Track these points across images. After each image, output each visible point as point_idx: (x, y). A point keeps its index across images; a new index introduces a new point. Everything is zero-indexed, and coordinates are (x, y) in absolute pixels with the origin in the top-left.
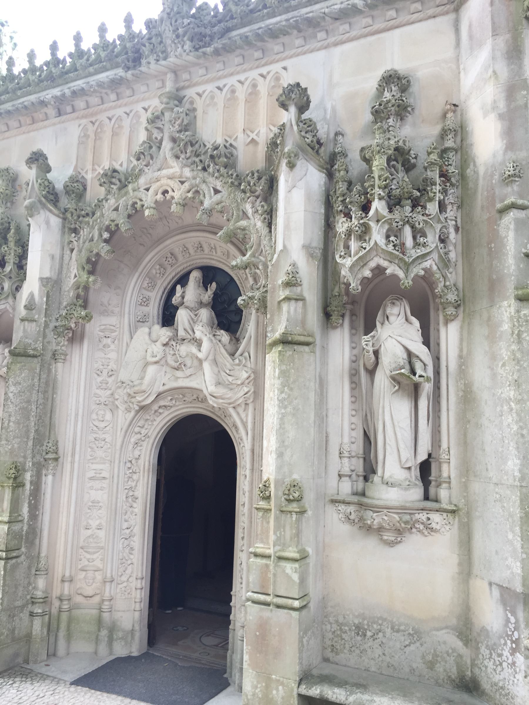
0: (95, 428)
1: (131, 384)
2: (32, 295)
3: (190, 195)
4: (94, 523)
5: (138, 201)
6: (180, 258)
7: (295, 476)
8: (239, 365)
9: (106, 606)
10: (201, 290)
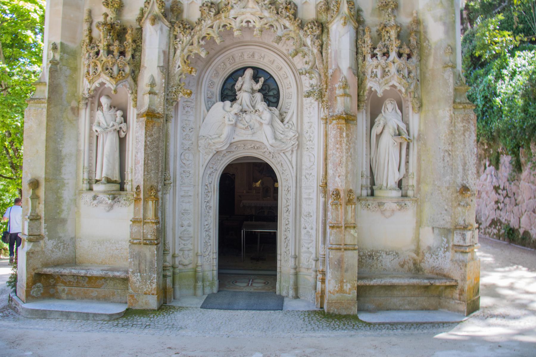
0: (183, 165)
1: (210, 137)
2: (152, 76)
3: (267, 26)
4: (186, 223)
5: (228, 25)
6: (237, 60)
7: (351, 188)
8: (287, 128)
9: (199, 269)
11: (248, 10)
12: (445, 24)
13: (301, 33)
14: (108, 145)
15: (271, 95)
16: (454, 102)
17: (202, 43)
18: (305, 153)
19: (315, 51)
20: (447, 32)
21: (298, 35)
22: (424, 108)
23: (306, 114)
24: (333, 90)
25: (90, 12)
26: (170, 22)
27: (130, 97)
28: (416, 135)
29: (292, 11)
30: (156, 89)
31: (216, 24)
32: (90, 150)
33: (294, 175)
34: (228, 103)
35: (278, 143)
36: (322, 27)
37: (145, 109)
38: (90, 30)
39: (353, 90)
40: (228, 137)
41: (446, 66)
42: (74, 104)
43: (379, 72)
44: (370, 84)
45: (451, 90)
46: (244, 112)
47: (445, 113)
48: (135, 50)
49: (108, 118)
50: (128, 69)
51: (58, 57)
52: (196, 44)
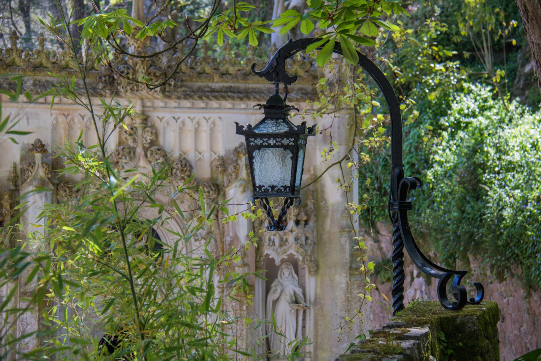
16: (351, 268)
22: (321, 271)
28: (312, 299)
36: (217, 188)
39: (251, 259)
41: (342, 230)
47: (341, 279)
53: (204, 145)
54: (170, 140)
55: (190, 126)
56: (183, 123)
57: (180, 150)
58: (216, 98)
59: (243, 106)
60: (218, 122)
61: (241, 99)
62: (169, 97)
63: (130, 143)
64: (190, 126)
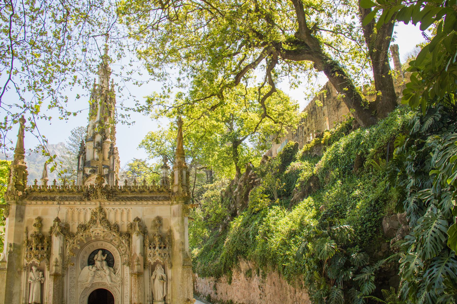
10: (102, 256)
11: (98, 228)
12: (180, 233)
13: (121, 238)
14: (35, 287)
15: (110, 262)
16: (183, 265)
17: (78, 243)
18: (125, 287)
19: (127, 246)
20: (181, 236)
21: (119, 239)
22: (173, 267)
23: (125, 270)
24: (133, 262)
25: (27, 228)
26: (64, 234)
27: (46, 266)
28: (170, 278)
29: (116, 229)
30: (58, 264)
31: (84, 234)
32: (26, 289)
33: (120, 296)
34: (91, 266)
35: (113, 283)
36: (129, 235)
37: (53, 272)
38: (27, 237)
39: (142, 262)
40: (91, 281)
41: (180, 251)
42: (19, 269)
43: (152, 254)
44: (149, 259)
45: (182, 260)
46: (98, 270)
47: (180, 269)
48: (48, 246)
49: (36, 275)
50: (45, 255)
51: (12, 250)
52: (75, 243)
53: (125, 219)
54: (111, 217)
55: (119, 212)
56: (117, 210)
57: (115, 220)
58: (129, 200)
59: (140, 203)
60: (131, 210)
61: (139, 201)
62: (110, 200)
63: (95, 218)
64: (119, 212)
